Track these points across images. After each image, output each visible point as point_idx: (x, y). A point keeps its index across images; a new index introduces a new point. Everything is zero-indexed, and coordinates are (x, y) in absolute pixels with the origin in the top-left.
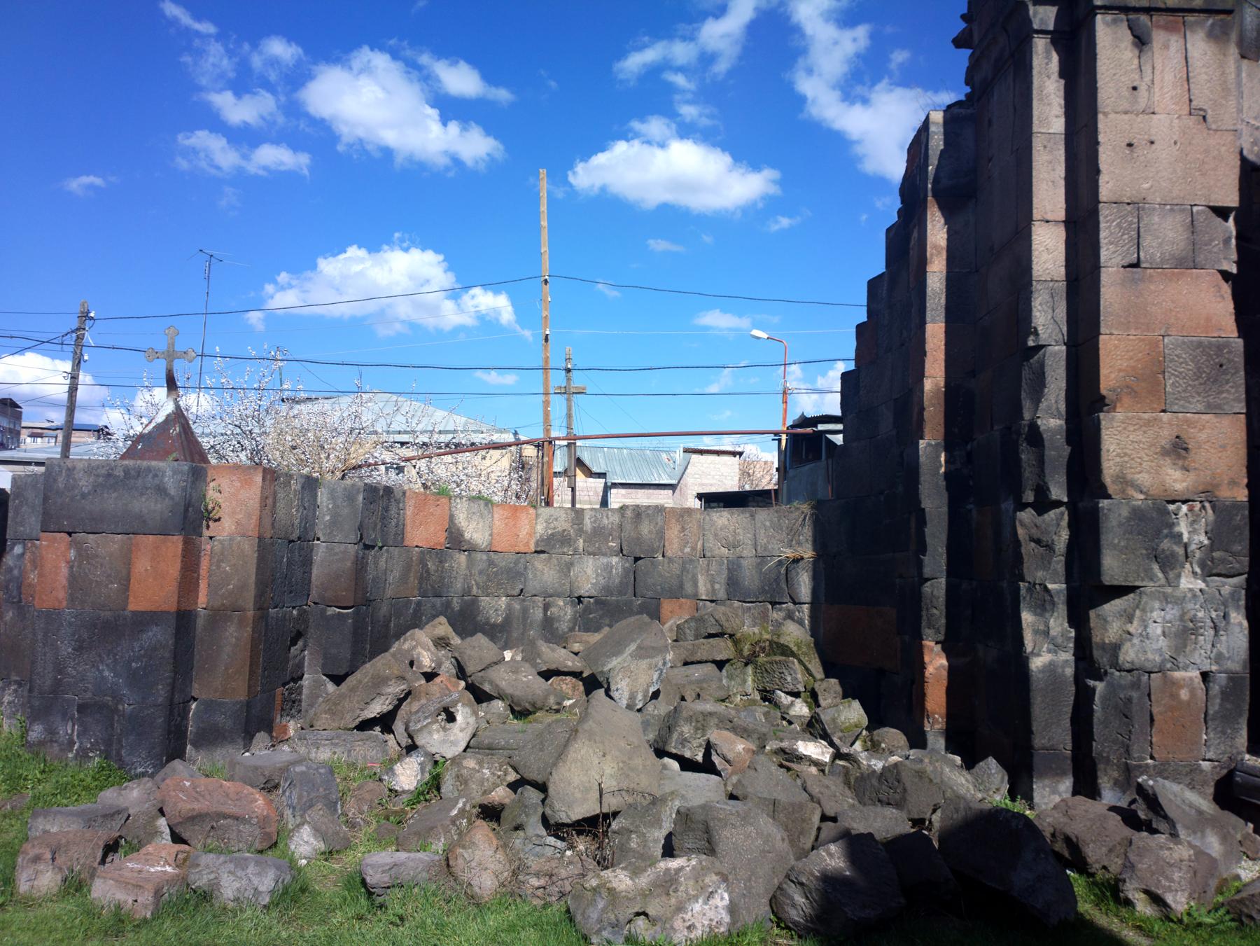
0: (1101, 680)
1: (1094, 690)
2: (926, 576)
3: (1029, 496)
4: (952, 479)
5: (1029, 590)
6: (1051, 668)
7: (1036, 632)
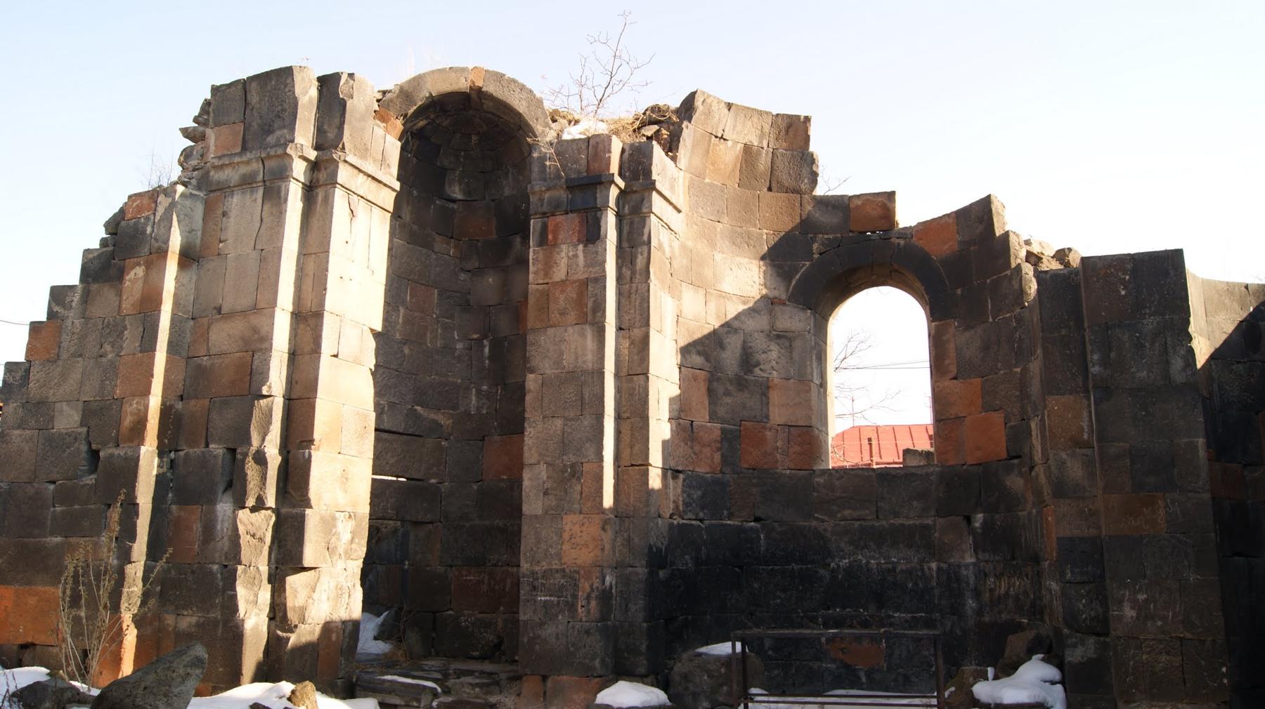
0: (292, 632)
1: (288, 639)
2: (306, 564)
3: (251, 502)
4: (160, 480)
5: (245, 572)
6: (256, 628)
7: (247, 601)
